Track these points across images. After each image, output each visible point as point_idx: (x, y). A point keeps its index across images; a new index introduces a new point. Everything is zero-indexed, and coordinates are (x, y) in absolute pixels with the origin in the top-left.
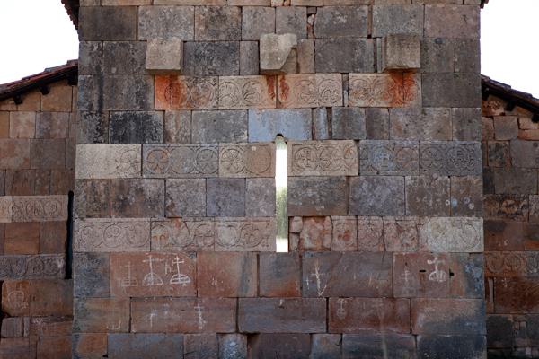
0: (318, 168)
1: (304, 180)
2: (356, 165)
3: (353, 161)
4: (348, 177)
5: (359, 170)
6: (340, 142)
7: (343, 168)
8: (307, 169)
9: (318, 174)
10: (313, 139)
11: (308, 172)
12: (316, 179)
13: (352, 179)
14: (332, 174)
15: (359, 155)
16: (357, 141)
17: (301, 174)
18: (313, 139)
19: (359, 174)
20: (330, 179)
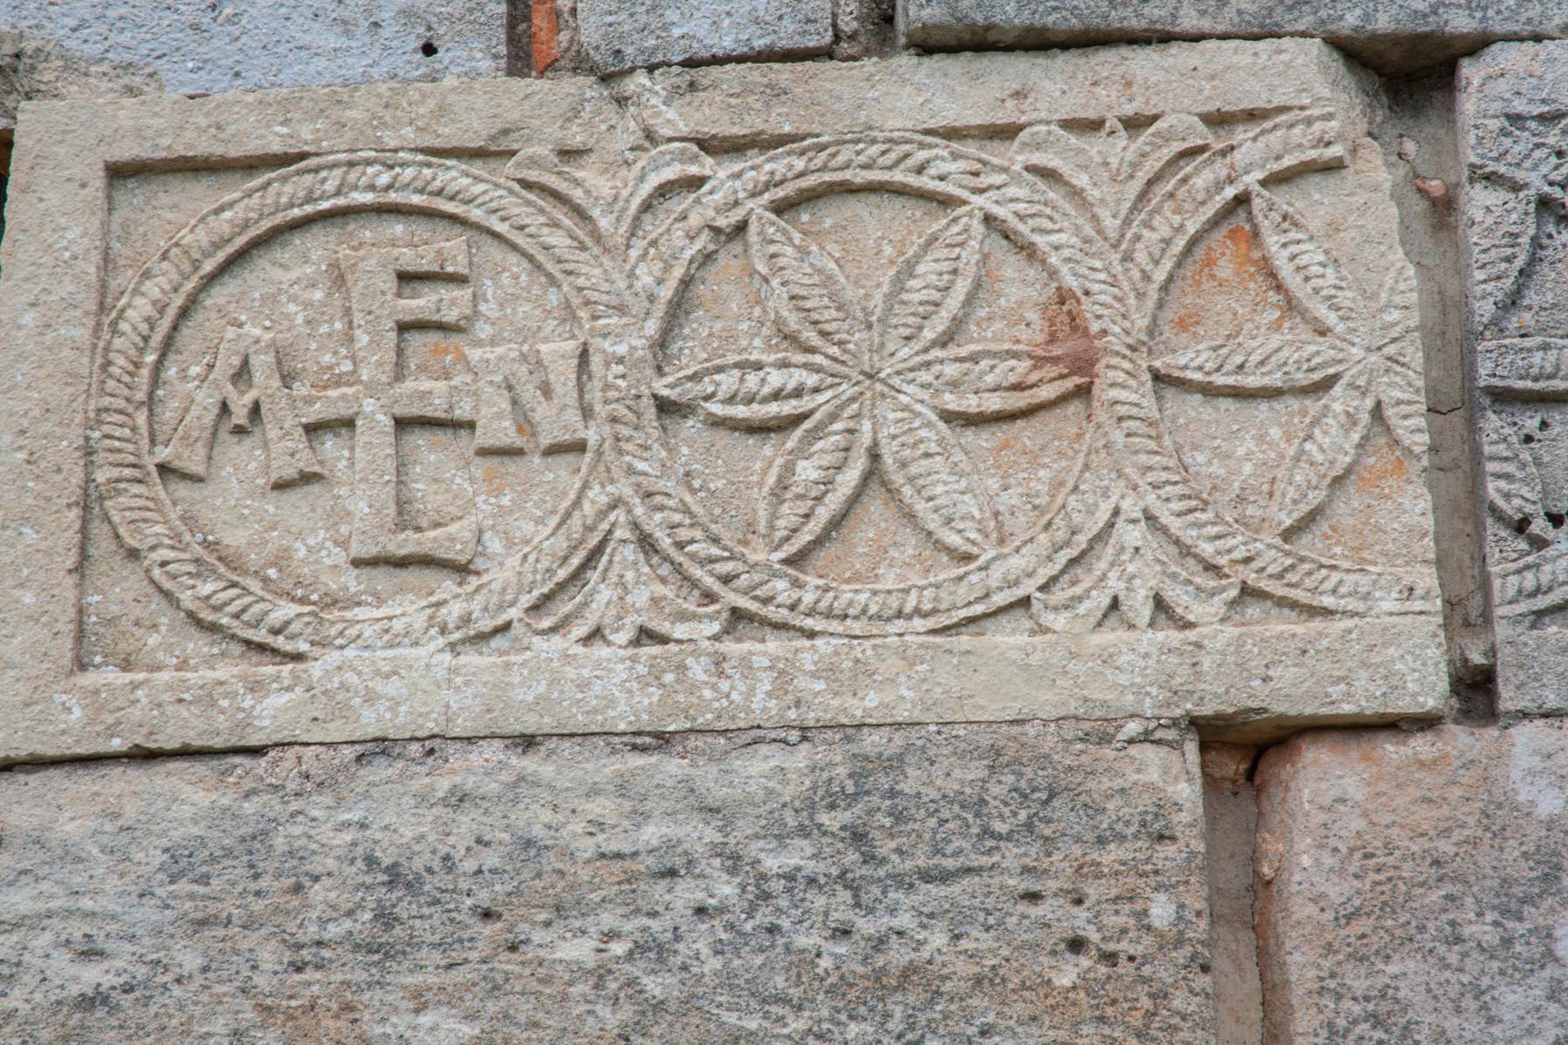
0: (628, 589)
1: (325, 828)
2: (1413, 507)
3: (1334, 438)
4: (1247, 751)
5: (1466, 611)
6: (1058, 85)
7: (1136, 572)
8: (406, 605)
9: (616, 686)
10: (522, 57)
11: (397, 663)
12: (577, 806)
13: (1320, 781)
14: (899, 685)
15: (1452, 334)
16: (1409, 75)
17: (273, 709)
18: (522, 57)
19: (1476, 691)
20: (867, 804)
